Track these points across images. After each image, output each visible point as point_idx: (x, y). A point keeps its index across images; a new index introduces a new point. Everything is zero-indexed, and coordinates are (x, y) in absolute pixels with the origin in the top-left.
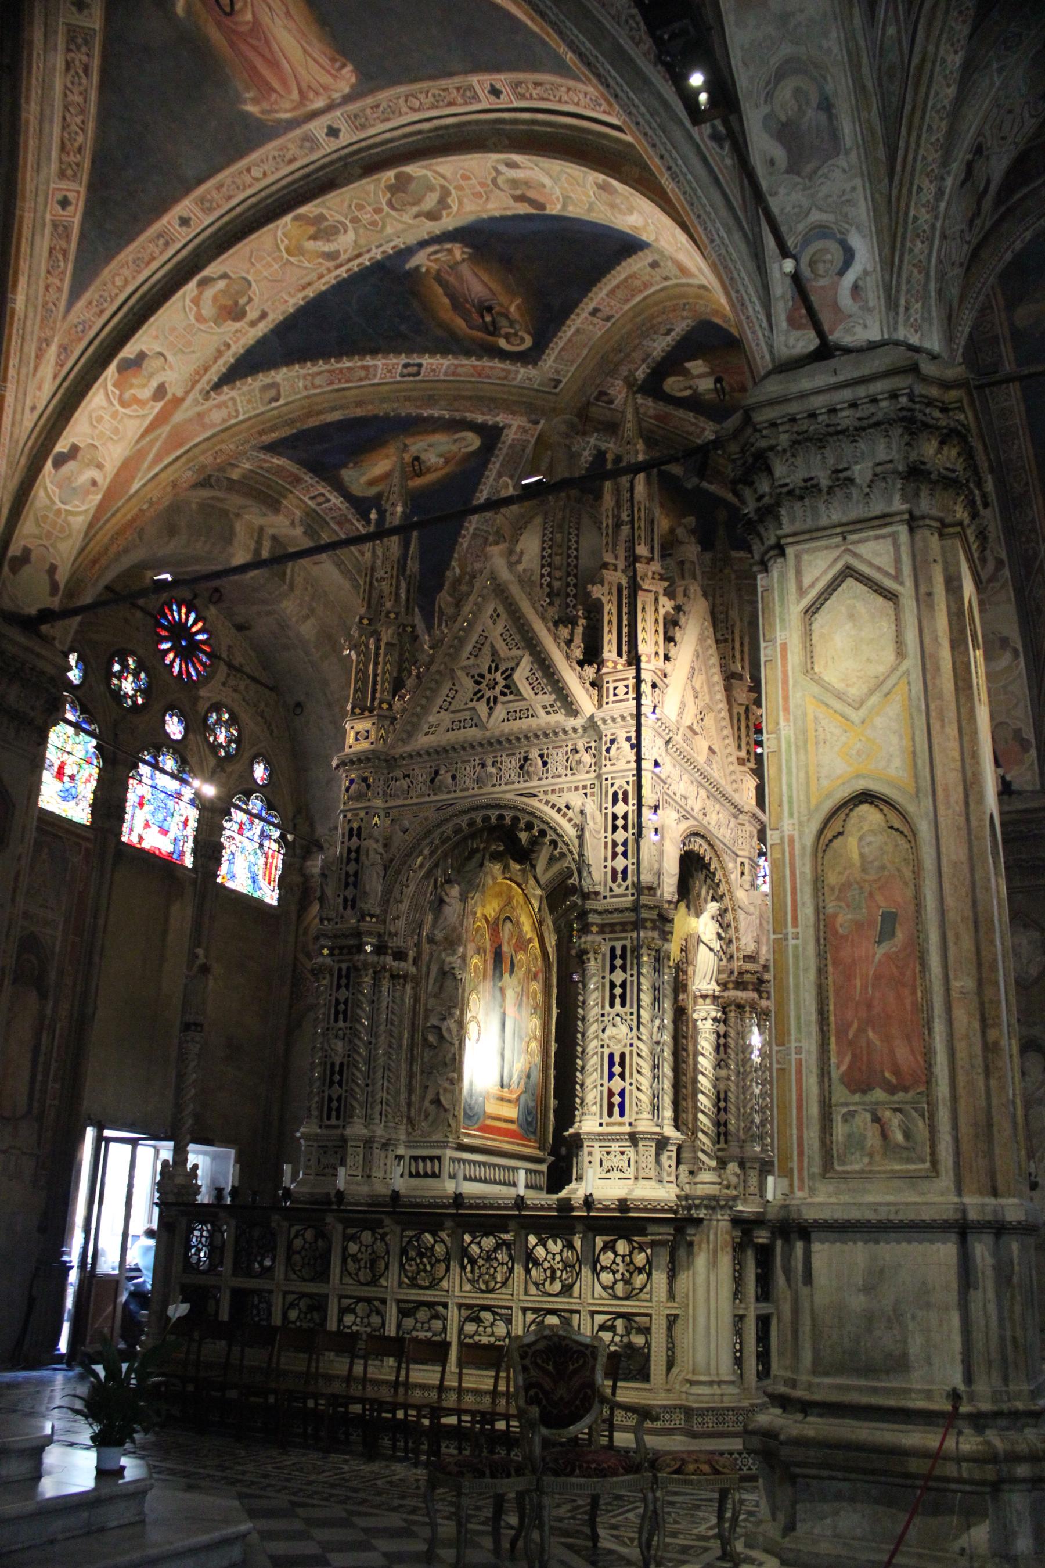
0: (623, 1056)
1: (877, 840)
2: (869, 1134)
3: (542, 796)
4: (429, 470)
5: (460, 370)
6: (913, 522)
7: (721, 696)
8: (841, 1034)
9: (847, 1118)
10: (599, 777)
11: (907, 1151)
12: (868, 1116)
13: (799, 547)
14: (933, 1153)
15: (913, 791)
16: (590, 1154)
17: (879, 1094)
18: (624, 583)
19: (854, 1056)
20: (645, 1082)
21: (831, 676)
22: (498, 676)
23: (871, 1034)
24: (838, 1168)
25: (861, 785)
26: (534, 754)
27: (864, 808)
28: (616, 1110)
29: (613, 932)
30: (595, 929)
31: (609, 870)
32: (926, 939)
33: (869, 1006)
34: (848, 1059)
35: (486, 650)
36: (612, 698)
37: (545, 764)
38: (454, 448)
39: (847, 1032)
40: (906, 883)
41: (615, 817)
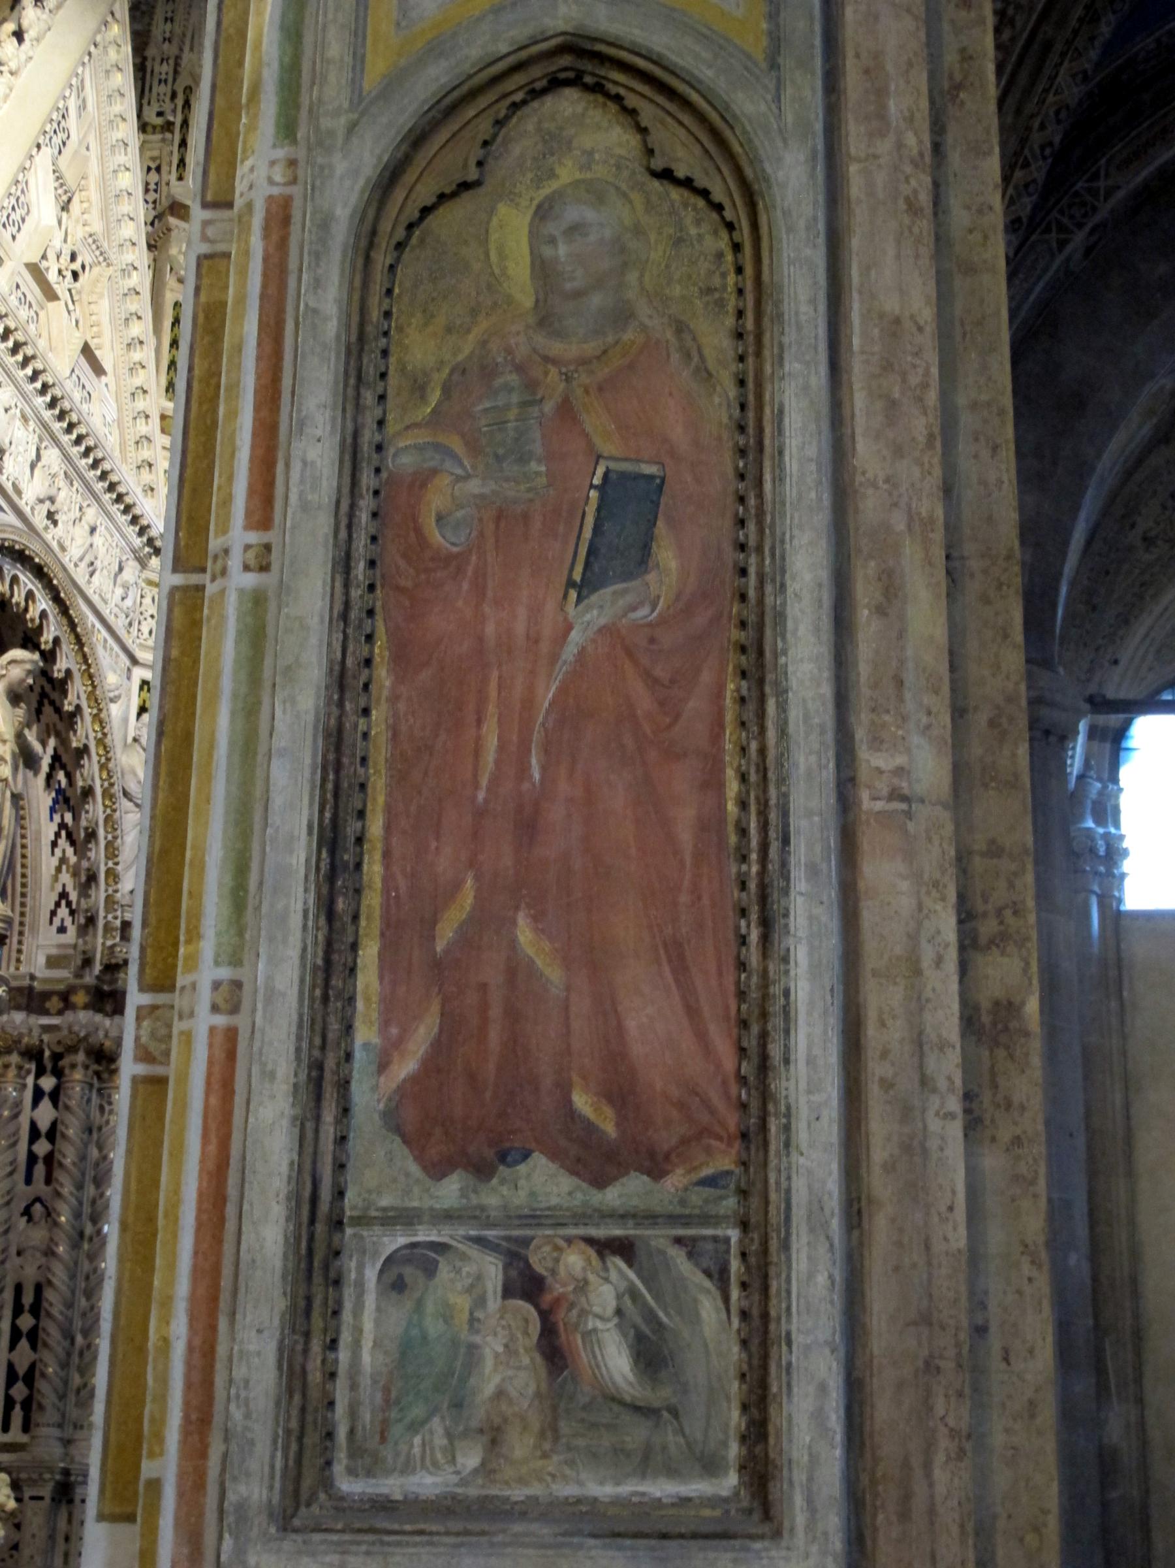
1: (603, 221)
2: (492, 1345)
7: (134, 230)
8: (408, 925)
9: (406, 1273)
11: (647, 1420)
12: (493, 1271)
14: (758, 1429)
15: (758, 48)
17: (543, 1181)
23: (525, 934)
24: (348, 1486)
27: (568, 104)
33: (528, 826)
34: (423, 1035)
39: (430, 925)
40: (705, 375)
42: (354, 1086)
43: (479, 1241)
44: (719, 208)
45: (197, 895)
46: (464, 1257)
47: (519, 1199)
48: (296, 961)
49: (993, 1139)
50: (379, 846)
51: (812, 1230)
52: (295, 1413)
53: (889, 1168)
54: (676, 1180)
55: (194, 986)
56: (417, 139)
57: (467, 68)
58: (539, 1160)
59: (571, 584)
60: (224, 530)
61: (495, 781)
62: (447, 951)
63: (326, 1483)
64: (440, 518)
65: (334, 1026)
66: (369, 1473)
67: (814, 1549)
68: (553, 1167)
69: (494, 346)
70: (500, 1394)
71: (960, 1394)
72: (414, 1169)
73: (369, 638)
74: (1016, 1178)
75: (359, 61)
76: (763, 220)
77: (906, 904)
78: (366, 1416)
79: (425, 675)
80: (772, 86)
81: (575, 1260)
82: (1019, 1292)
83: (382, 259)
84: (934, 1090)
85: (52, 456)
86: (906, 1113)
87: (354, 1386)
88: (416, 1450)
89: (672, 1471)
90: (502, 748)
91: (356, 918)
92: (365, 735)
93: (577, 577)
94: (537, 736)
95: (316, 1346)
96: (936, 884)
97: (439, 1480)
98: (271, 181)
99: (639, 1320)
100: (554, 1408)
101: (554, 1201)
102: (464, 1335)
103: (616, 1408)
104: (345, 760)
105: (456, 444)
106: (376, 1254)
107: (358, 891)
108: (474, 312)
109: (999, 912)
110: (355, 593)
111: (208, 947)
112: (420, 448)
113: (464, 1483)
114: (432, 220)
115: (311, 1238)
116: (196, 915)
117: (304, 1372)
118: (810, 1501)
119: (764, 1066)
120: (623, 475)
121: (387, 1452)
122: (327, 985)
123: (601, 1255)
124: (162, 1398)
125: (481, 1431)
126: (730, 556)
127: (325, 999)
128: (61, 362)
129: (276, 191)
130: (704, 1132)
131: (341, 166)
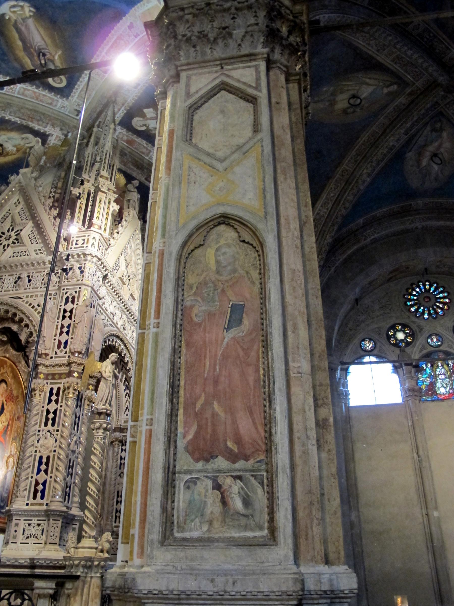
0: (48, 458)
1: (230, 251)
2: (210, 501)
3: (24, 299)
4: (7, 154)
5: (26, 92)
6: (270, 64)
10: (59, 287)
11: (246, 518)
12: (210, 484)
13: (190, 73)
14: (272, 520)
15: (262, 215)
16: (17, 525)
17: (221, 463)
18: (92, 191)
19: (198, 425)
20: (60, 478)
21: (205, 145)
22: (13, 234)
23: (216, 405)
24: (177, 535)
25: (221, 210)
26: (24, 276)
27: (222, 228)
28: (39, 494)
29: (53, 378)
30: (42, 376)
31: (57, 342)
32: (270, 325)
33: (216, 382)
34: (194, 429)
35: (9, 220)
36: (74, 245)
37: (30, 281)
38: (22, 143)
39: (194, 404)
40: (253, 283)
41: (65, 311)
42: (178, 442)
43: (207, 477)
44: (255, 248)
45: (143, 400)
46: (203, 480)
47: (216, 467)
48: (164, 414)
49: (324, 450)
50: (183, 387)
51: (283, 472)
52: (164, 518)
53: (300, 457)
54: (251, 462)
55: (142, 420)
56: (190, 236)
57: (201, 221)
58: (220, 458)
59: (225, 328)
60: (149, 320)
61: (209, 371)
62: (198, 411)
63: (172, 534)
64: (196, 315)
65: (173, 428)
66: (182, 532)
67: (286, 548)
68: (223, 459)
69: (207, 278)
70: (212, 512)
71: (319, 510)
72: (192, 461)
73: (181, 341)
74: (329, 459)
75: (178, 220)
76: (264, 250)
77: (302, 397)
78: (181, 518)
79: (193, 350)
80: (265, 222)
81: (229, 481)
82: (331, 485)
83: (183, 261)
84: (310, 439)
85: (124, 316)
86: (304, 445)
87: (178, 511)
88: (193, 526)
89: (252, 530)
90: (210, 365)
91: (178, 403)
92: (180, 363)
93: (226, 327)
94: (218, 361)
95: (169, 502)
96: (308, 392)
97: (198, 533)
98: (160, 246)
99: (244, 495)
100: (225, 515)
101: (224, 467)
102: (203, 499)
103: (239, 515)
104: (175, 368)
105: (200, 300)
106: (183, 480)
107: (178, 397)
108: (203, 271)
109: (323, 399)
110: (177, 332)
111: (145, 411)
112: (191, 300)
113: (204, 534)
114: (193, 253)
115: (168, 477)
116: (143, 404)
117: (166, 508)
118: (284, 537)
119: (271, 435)
120: (236, 304)
121: (186, 527)
122: (171, 419)
123: (235, 480)
124: (135, 515)
125: (208, 521)
126: (260, 321)
127: (171, 422)
128: (126, 297)
129: (161, 248)
130: (257, 450)
131: (174, 242)
